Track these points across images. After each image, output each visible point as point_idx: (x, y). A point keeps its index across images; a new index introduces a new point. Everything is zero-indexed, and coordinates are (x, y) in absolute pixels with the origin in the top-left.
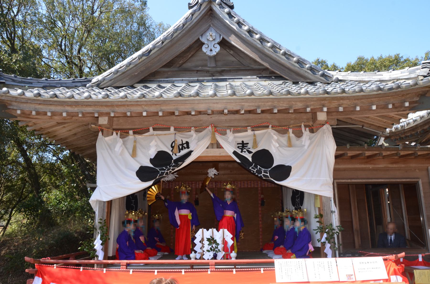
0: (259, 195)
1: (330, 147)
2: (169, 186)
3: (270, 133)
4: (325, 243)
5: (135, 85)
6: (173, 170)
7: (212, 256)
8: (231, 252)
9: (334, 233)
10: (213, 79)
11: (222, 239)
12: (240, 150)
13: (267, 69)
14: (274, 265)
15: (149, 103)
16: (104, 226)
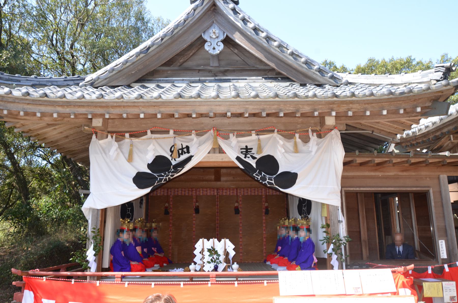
0: (264, 204)
1: (338, 153)
2: (167, 193)
3: (275, 138)
4: (331, 254)
5: (132, 85)
6: (172, 176)
7: (213, 268)
8: (233, 263)
9: (341, 243)
10: (216, 80)
12: (244, 156)
13: (273, 70)
15: (147, 104)
16: (98, 235)
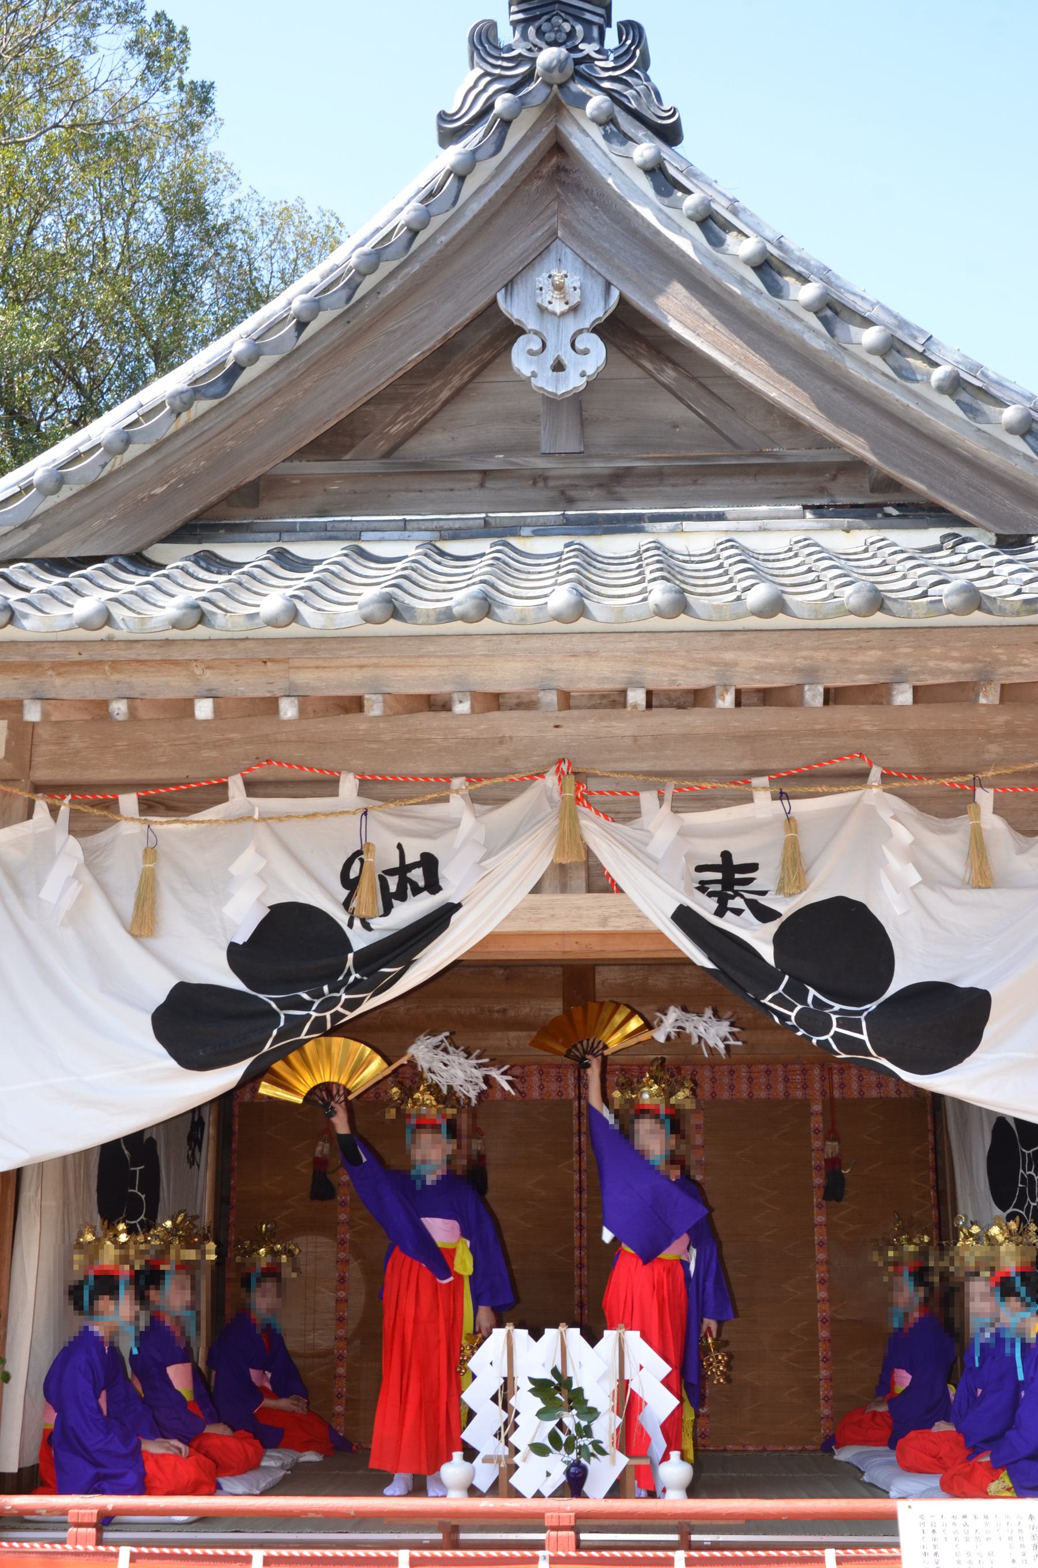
0: (817, 1144)
3: (871, 811)
5: (157, 552)
6: (351, 1005)
7: (559, 1477)
10: (568, 521)
11: (612, 1385)
12: (713, 904)
13: (856, 466)
14: (895, 1532)
15: (230, 653)
